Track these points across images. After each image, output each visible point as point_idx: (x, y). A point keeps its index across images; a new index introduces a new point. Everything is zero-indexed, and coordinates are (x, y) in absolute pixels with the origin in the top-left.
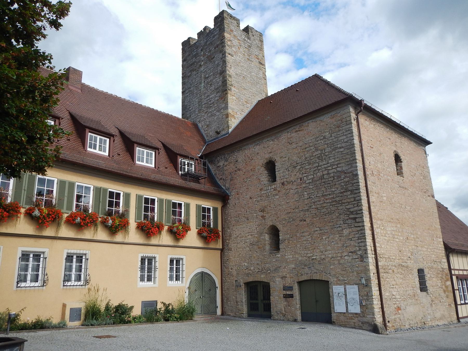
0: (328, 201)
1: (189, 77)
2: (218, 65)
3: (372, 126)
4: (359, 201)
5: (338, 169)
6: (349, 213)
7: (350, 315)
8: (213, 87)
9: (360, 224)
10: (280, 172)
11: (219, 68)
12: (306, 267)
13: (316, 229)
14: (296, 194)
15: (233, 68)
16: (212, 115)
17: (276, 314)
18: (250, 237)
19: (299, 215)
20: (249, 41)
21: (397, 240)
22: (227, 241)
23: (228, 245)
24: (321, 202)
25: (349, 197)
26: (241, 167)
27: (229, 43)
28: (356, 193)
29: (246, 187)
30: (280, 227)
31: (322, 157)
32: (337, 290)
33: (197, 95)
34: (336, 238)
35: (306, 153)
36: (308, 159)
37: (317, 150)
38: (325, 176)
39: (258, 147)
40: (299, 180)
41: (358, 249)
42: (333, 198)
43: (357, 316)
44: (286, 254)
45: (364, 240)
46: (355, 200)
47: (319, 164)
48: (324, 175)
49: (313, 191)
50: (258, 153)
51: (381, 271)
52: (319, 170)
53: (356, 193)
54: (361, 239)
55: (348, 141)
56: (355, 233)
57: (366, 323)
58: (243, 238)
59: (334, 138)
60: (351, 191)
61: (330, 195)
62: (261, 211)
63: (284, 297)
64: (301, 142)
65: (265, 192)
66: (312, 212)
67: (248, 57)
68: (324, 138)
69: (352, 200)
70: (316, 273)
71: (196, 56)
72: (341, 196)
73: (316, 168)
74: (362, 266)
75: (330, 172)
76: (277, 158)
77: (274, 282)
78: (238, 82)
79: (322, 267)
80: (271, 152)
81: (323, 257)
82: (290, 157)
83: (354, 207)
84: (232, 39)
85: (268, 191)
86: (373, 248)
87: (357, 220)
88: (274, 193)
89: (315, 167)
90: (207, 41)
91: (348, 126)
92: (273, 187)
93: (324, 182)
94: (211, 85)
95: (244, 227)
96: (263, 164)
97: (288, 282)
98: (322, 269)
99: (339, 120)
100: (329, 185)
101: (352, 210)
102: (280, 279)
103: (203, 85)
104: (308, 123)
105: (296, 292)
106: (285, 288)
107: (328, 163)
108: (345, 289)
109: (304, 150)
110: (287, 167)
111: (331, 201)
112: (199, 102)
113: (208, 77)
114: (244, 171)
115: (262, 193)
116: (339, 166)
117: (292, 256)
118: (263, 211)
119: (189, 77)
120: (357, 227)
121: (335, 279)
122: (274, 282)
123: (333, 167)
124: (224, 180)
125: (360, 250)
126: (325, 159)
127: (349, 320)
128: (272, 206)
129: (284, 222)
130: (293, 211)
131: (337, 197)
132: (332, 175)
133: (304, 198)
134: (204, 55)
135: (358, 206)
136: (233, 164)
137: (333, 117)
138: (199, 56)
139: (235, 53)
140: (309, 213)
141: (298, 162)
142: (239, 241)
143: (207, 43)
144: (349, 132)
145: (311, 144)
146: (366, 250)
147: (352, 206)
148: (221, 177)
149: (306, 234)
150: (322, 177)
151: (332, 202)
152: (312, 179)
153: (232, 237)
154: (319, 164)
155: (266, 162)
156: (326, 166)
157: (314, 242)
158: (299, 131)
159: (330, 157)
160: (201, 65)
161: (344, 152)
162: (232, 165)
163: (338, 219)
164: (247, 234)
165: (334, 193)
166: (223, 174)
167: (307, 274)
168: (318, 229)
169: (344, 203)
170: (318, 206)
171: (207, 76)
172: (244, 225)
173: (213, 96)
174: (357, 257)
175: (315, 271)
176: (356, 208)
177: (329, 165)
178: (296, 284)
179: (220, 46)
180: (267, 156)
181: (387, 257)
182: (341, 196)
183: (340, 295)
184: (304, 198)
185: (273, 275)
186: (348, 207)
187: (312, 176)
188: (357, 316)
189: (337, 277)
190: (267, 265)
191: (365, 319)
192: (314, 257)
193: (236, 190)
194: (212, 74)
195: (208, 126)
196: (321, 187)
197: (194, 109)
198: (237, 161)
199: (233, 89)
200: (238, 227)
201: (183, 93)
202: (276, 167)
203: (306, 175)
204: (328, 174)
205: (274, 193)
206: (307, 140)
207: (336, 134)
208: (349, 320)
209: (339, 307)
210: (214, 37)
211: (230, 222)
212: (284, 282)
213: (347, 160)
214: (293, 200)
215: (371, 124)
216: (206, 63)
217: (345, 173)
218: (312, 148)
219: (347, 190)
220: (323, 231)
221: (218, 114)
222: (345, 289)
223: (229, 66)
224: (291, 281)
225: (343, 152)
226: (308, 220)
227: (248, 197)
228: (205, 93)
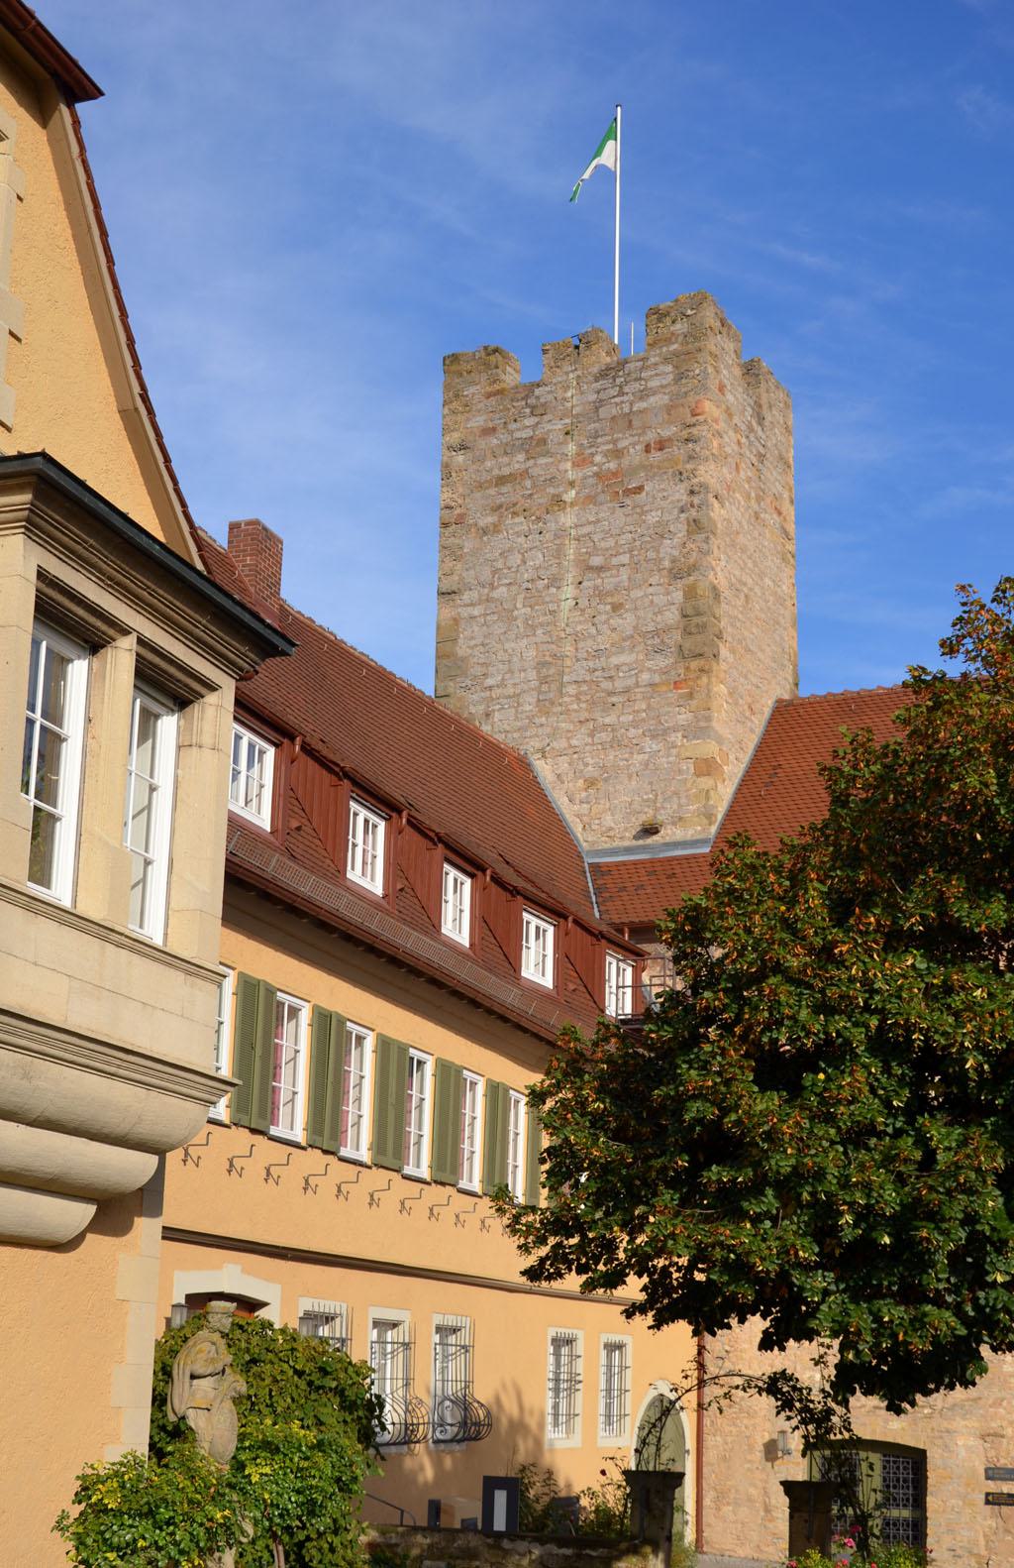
2: (661, 533)
8: (630, 618)
11: (669, 549)
16: (616, 743)
17: (947, 1555)
33: (533, 628)
63: (988, 1502)
94: (616, 607)
102: (972, 1442)
103: (569, 591)
112: (541, 665)
113: (600, 569)
134: (581, 461)
138: (547, 453)
143: (603, 412)
160: (558, 502)
171: (596, 561)
179: (678, 451)
185: (945, 1425)
194: (625, 559)
195: (591, 783)
197: (511, 691)
199: (724, 652)
210: (643, 395)
212: (992, 1453)
221: (650, 745)
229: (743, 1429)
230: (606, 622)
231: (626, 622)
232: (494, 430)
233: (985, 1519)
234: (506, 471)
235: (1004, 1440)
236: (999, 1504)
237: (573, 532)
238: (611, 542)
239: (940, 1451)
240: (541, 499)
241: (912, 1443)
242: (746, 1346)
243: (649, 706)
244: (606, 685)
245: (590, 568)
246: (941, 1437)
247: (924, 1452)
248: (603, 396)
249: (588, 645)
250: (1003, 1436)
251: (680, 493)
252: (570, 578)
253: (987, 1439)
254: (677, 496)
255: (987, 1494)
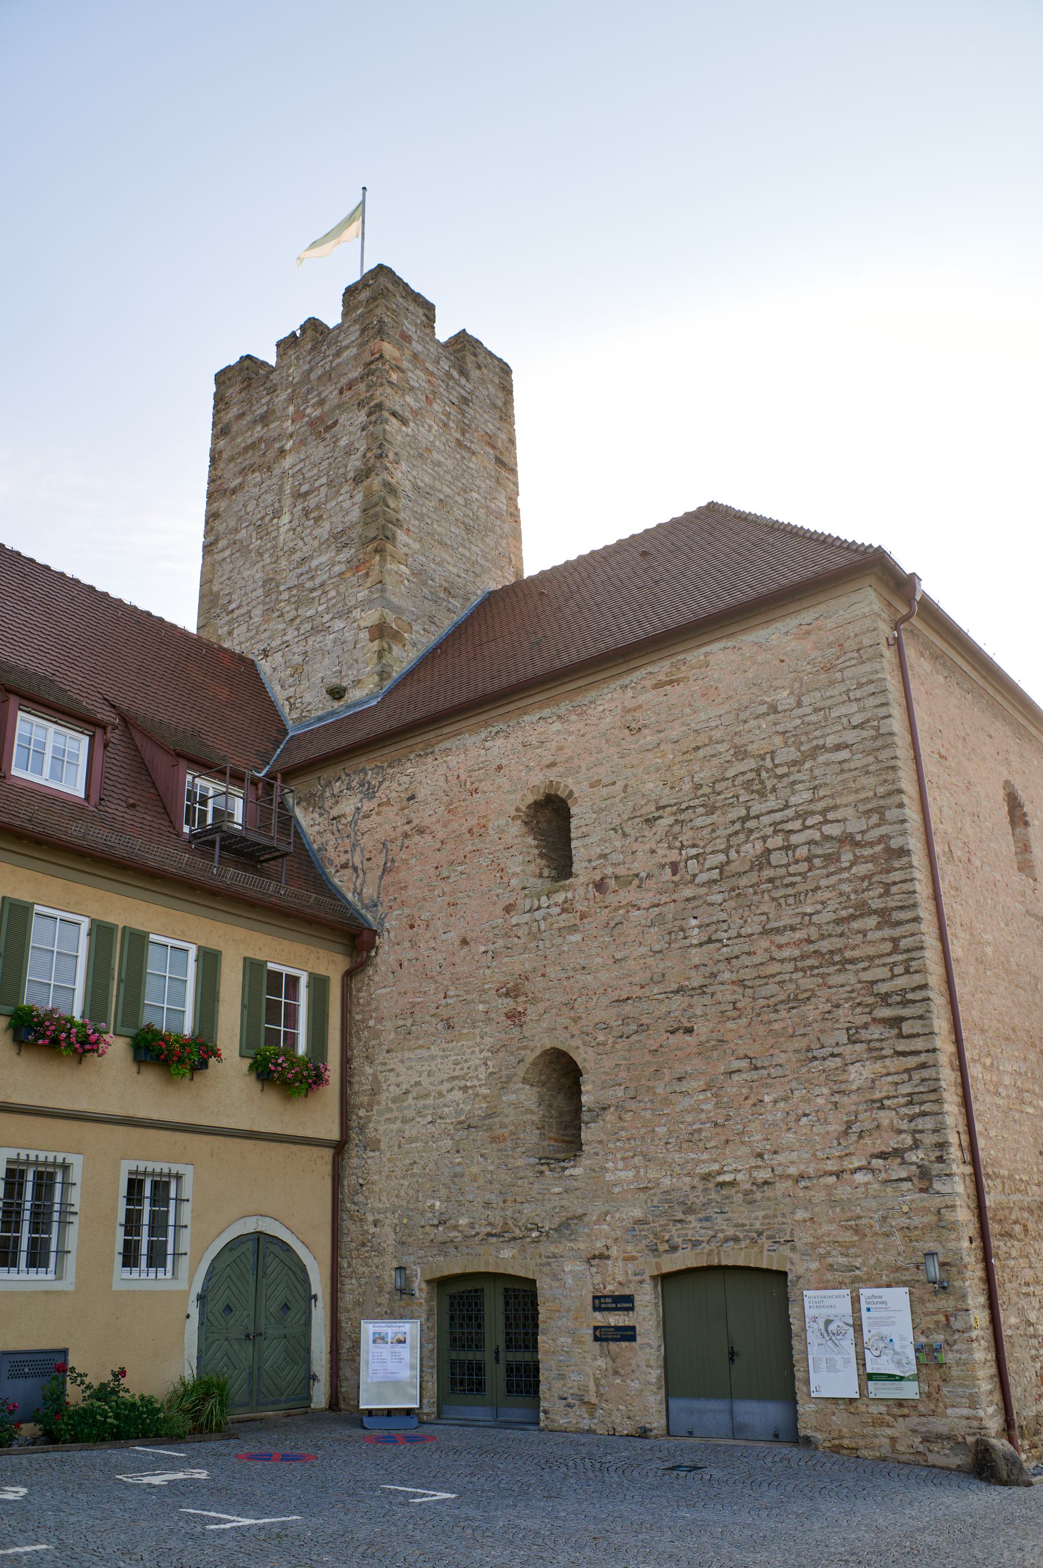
0: (786, 953)
1: (234, 491)
3: (941, 679)
4: (914, 955)
5: (828, 830)
6: (871, 1000)
7: (874, 1409)
8: (326, 525)
9: (919, 1044)
10: (588, 841)
11: (355, 462)
12: (691, 1218)
13: (736, 1064)
14: (652, 924)
15: (404, 466)
16: (315, 630)
18: (457, 1095)
19: (663, 1009)
20: (463, 381)
21: (1031, 1110)
22: (362, 1113)
23: (362, 1129)
24: (757, 959)
25: (870, 936)
26: (427, 822)
27: (394, 377)
28: (899, 923)
29: (447, 899)
30: (583, 1057)
31: (762, 782)
32: (819, 1307)
33: (261, 555)
34: (820, 1101)
35: (696, 767)
36: (706, 790)
37: (741, 753)
38: (776, 858)
39: (500, 741)
40: (668, 870)
41: (909, 1141)
42: (809, 941)
43: (906, 1411)
44: (610, 1165)
45: (935, 1108)
46: (895, 950)
47: (748, 809)
48: (769, 851)
49: (723, 916)
50: (500, 768)
51: (994, 1228)
52: (751, 831)
53: (899, 923)
54: (922, 1103)
55: (868, 721)
56: (896, 1078)
57: (940, 1437)
58: (430, 1101)
59: (808, 710)
60: (883, 914)
61: (793, 929)
62: (507, 995)
63: (596, 1339)
64: (676, 724)
65: (526, 917)
66: (719, 996)
67: (458, 436)
68: (774, 709)
69: (888, 947)
70: (736, 1239)
71: (264, 419)
72: (841, 935)
73: (738, 826)
74: (926, 1210)
75: (794, 839)
76: (574, 786)
77: (555, 1277)
78: (420, 517)
79: (761, 1214)
80: (553, 764)
81: (763, 1175)
82: (632, 782)
83: (893, 976)
84: (405, 364)
85: (538, 915)
86: (965, 1138)
87: (907, 1028)
88: (565, 920)
89: (733, 822)
90: (311, 370)
91: (867, 668)
92: (560, 897)
93: (771, 880)
94: (317, 519)
95: (433, 1057)
96: (518, 810)
97: (616, 1277)
98: (758, 1225)
99: (830, 645)
100: (790, 891)
101: (883, 988)
102: (580, 1267)
103: (286, 518)
104: (706, 655)
105: (646, 1316)
106: (601, 1303)
107: (787, 806)
108: (856, 1301)
109: (688, 757)
110: (617, 821)
111: (797, 953)
112: (266, 582)
114: (441, 835)
115: (514, 921)
116: (830, 816)
117: (631, 1174)
118: (512, 993)
119: (234, 491)
120: (904, 1054)
121: (814, 1266)
122: (555, 1277)
123: (809, 822)
124: (356, 869)
125: (916, 1145)
126: (774, 790)
127: (869, 1430)
128: (552, 972)
129: (601, 1038)
130: (640, 993)
131: (822, 937)
132: (802, 852)
133: (687, 942)
134: (299, 415)
135: (907, 971)
136: (395, 809)
137: (808, 633)
138: (278, 419)
139: (415, 413)
140: (707, 1000)
141: (662, 803)
142: (410, 1113)
144: (871, 688)
145: (717, 735)
146: (942, 1146)
147: (885, 972)
148: (343, 858)
149: (694, 1084)
150: (763, 860)
151: (803, 957)
152: (721, 867)
153: (384, 1096)
154: (748, 809)
155: (530, 799)
156: (778, 816)
157: (728, 1118)
158: (671, 682)
159: (794, 783)
160: (282, 452)
161: (853, 766)
162: (390, 812)
163: (829, 1024)
164: (446, 1086)
165: (810, 923)
166: (354, 846)
167: (695, 1244)
168: (744, 1064)
169: (851, 961)
170: (748, 974)
171: (304, 488)
172: (434, 1050)
173: (323, 559)
174: (904, 1175)
175: (731, 1232)
176: (901, 982)
177: (790, 813)
178: (648, 1287)
180: (538, 780)
181: (1006, 1173)
182: (841, 935)
183: (832, 1327)
184: (687, 942)
185: (553, 1248)
186: (868, 976)
187: (722, 858)
188: (906, 1411)
189: (822, 1257)
190: (527, 1210)
191: (939, 1425)
192: (728, 1178)
193: (407, 911)
194: (323, 480)
196: (756, 898)
198: (412, 798)
199: (401, 537)
200: (407, 1055)
201: (208, 549)
202: (574, 823)
203: (693, 852)
204: (787, 848)
205: (565, 920)
206: (703, 716)
207: (817, 694)
208: (869, 1430)
209: (828, 1375)
210: (338, 354)
211: (377, 1035)
212: (598, 1279)
213: (862, 795)
214: (643, 950)
215: (937, 673)
216: (303, 442)
217: (858, 844)
218: (721, 748)
219: (863, 910)
220: (764, 1072)
221: (338, 624)
222: (856, 1301)
223: (391, 455)
224: (630, 1271)
225: (845, 766)
226: (702, 1029)
227: (454, 936)
228: (293, 551)
229: (374, 1268)
230: (310, 534)
231: (324, 530)
232: (243, 414)
233: (595, 1359)
234: (249, 441)
235: (610, 1262)
236: (607, 1340)
237: (290, 472)
238: (316, 471)
239: (549, 1280)
240: (271, 454)
241: (522, 1274)
242: (376, 1177)
243: (338, 594)
244: (309, 585)
245: (299, 495)
246: (549, 1264)
247: (533, 1282)
248: (313, 363)
249: (297, 557)
250: (608, 1257)
251: (362, 417)
252: (286, 509)
253: (593, 1262)
254: (360, 420)
255: (596, 1328)
